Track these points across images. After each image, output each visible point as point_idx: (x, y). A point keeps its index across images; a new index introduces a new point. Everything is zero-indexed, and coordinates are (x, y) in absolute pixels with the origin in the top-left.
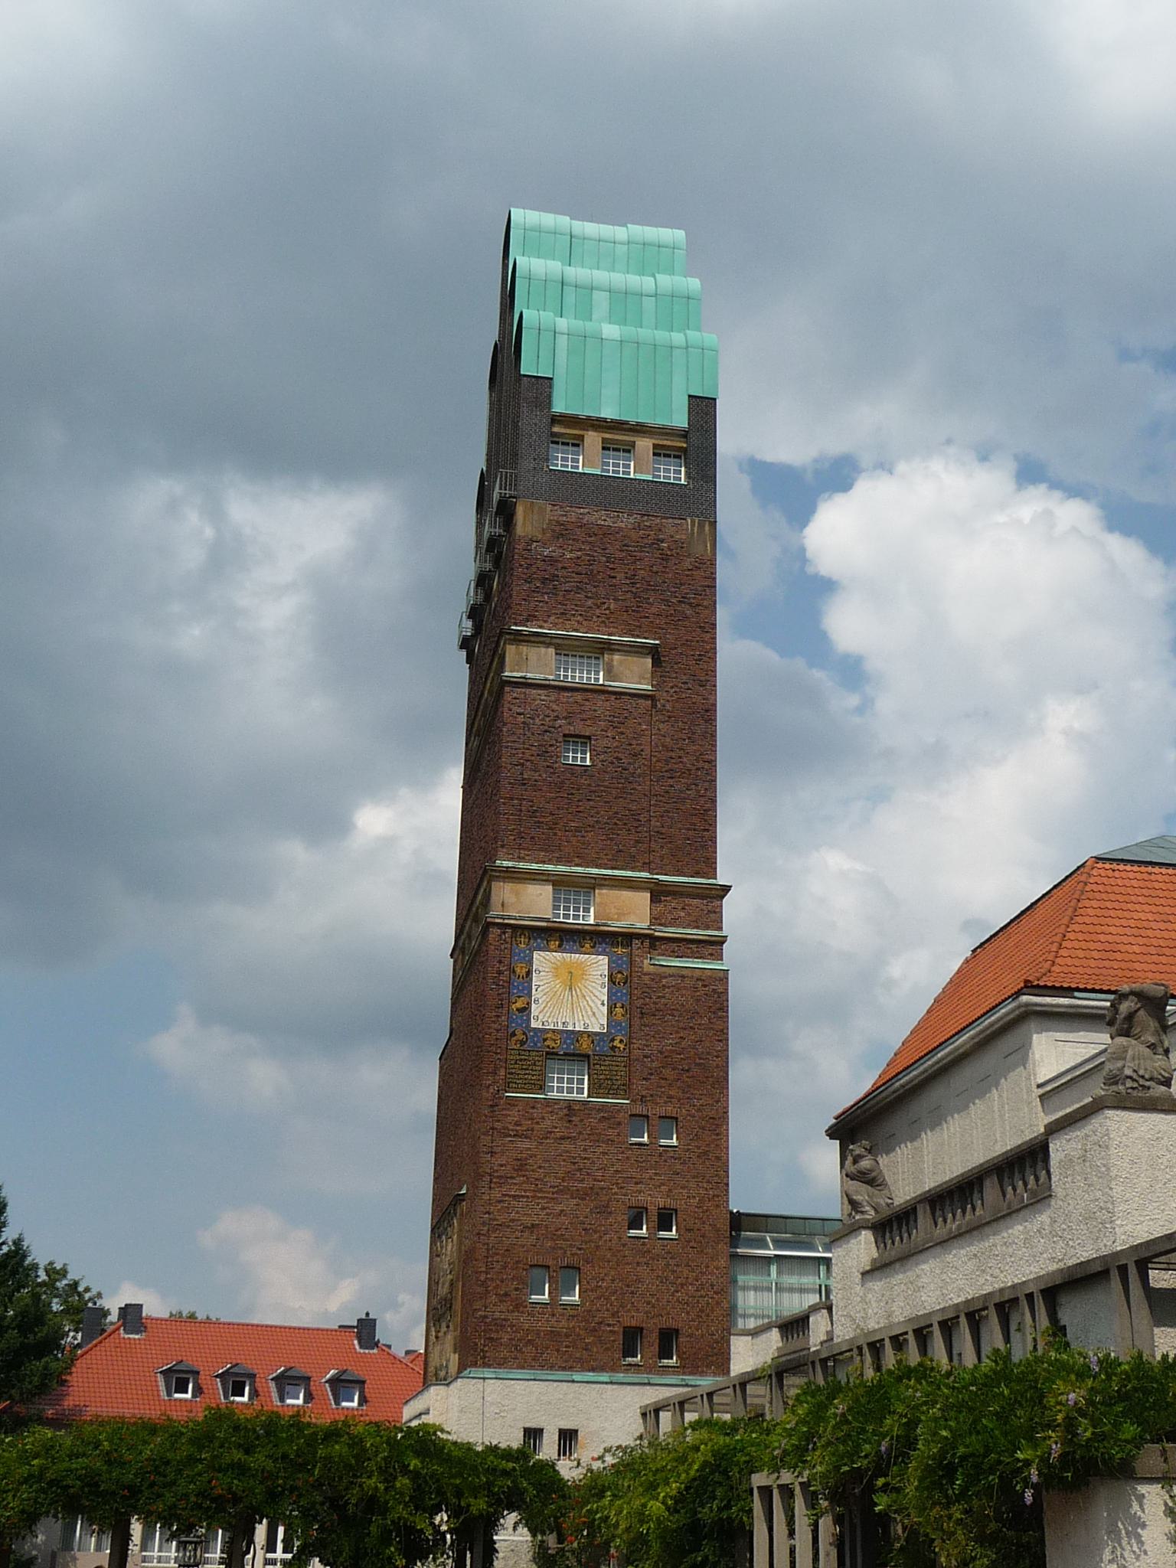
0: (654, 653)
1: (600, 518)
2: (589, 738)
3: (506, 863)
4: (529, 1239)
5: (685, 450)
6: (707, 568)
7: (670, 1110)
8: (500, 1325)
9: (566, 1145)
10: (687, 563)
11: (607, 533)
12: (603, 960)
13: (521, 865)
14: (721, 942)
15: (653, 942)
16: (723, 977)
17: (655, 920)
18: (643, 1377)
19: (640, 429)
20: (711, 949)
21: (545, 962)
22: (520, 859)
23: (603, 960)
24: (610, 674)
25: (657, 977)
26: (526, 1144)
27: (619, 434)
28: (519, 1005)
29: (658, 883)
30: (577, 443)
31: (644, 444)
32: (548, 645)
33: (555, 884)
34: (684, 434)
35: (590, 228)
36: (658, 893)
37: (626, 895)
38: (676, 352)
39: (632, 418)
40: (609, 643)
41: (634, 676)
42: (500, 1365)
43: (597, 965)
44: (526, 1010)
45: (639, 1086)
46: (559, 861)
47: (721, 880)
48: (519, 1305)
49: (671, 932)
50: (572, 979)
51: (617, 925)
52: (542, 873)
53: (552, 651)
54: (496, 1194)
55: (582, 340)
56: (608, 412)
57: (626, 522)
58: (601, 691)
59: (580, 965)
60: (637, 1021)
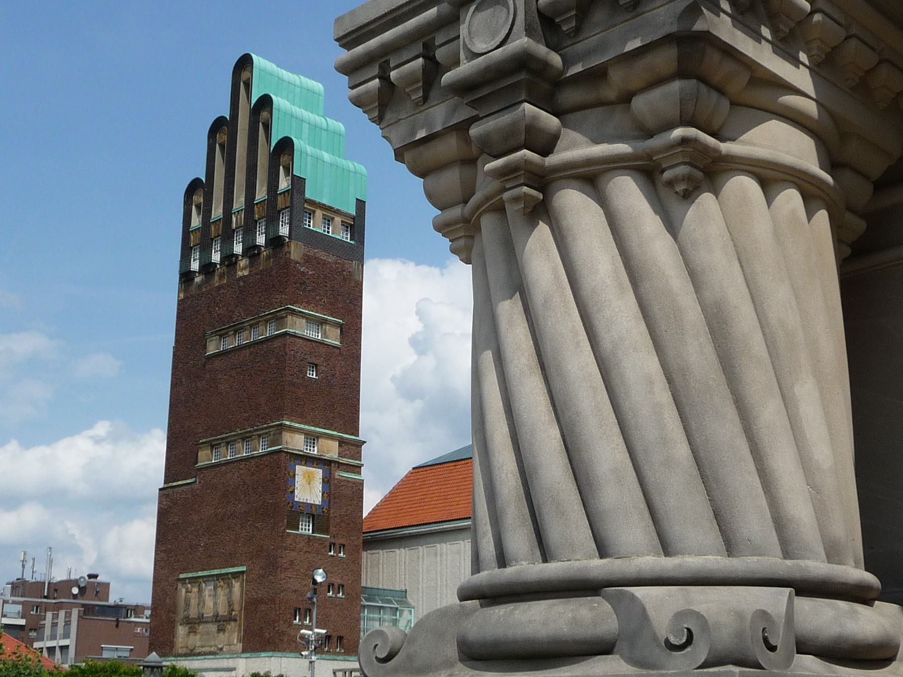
0: (341, 326)
1: (322, 255)
2: (316, 365)
3: (288, 423)
4: (294, 597)
5: (351, 225)
6: (359, 285)
7: (342, 541)
8: (283, 633)
9: (307, 555)
10: (352, 284)
11: (325, 263)
12: (321, 471)
13: (293, 424)
14: (359, 467)
15: (339, 465)
16: (360, 484)
17: (340, 455)
18: (331, 657)
19: (338, 212)
20: (357, 469)
21: (300, 469)
22: (292, 421)
23: (321, 471)
24: (325, 334)
25: (340, 481)
26: (293, 554)
27: (330, 212)
28: (291, 490)
29: (342, 438)
30: (312, 214)
31: (338, 220)
32: (303, 317)
33: (305, 434)
34: (354, 219)
35: (286, 74)
36: (342, 442)
37: (330, 442)
38: (352, 174)
39: (336, 207)
40: (326, 320)
41: (333, 339)
42: (284, 650)
43: (318, 473)
44: (293, 492)
45: (332, 529)
46: (305, 423)
47: (361, 438)
48: (291, 625)
49: (345, 460)
50: (309, 479)
51: (327, 456)
52: (302, 429)
53: (304, 321)
54: (283, 576)
55: (317, 159)
56: (325, 201)
57: (331, 259)
58: (321, 343)
59: (312, 473)
60: (332, 500)
